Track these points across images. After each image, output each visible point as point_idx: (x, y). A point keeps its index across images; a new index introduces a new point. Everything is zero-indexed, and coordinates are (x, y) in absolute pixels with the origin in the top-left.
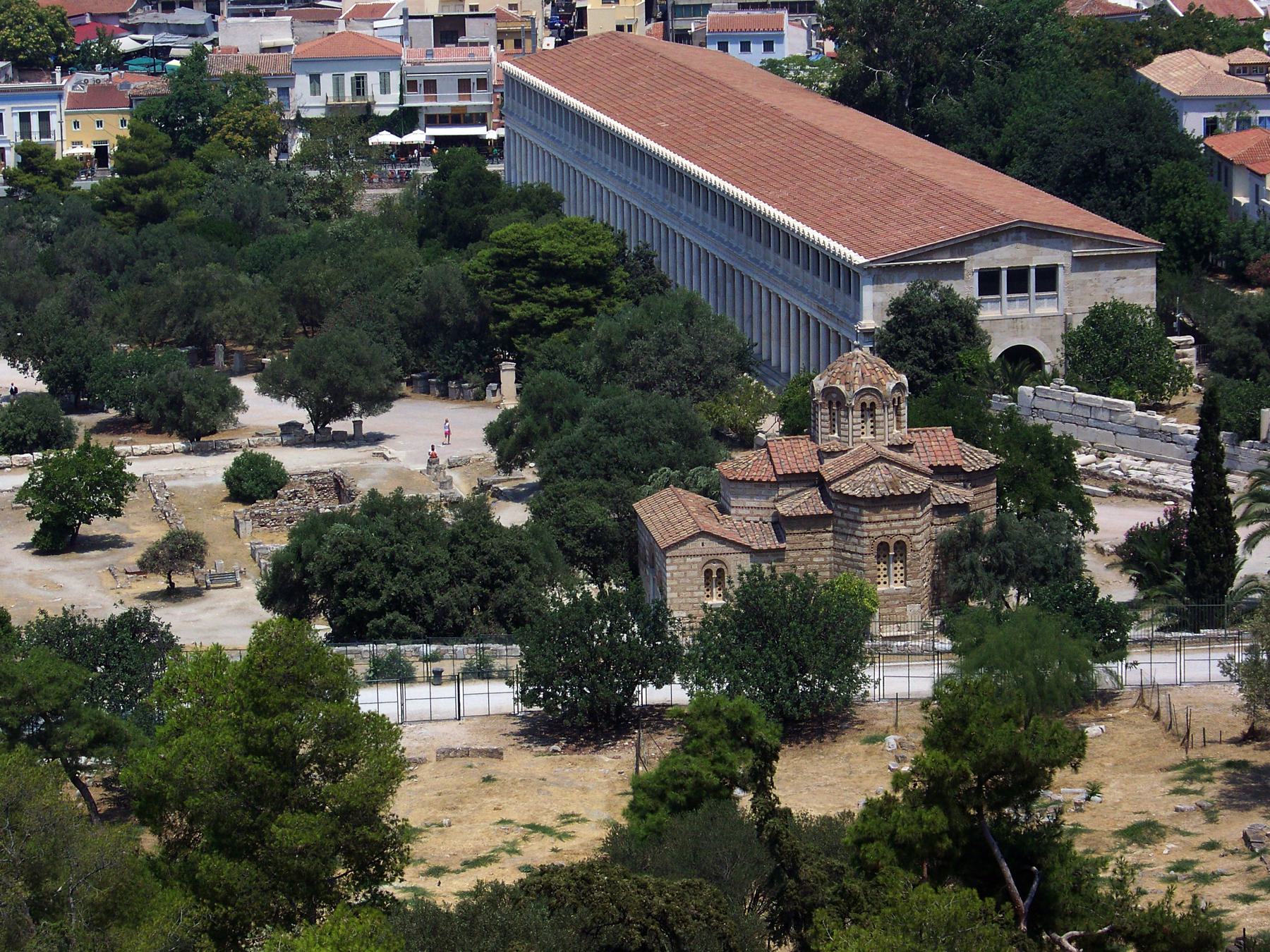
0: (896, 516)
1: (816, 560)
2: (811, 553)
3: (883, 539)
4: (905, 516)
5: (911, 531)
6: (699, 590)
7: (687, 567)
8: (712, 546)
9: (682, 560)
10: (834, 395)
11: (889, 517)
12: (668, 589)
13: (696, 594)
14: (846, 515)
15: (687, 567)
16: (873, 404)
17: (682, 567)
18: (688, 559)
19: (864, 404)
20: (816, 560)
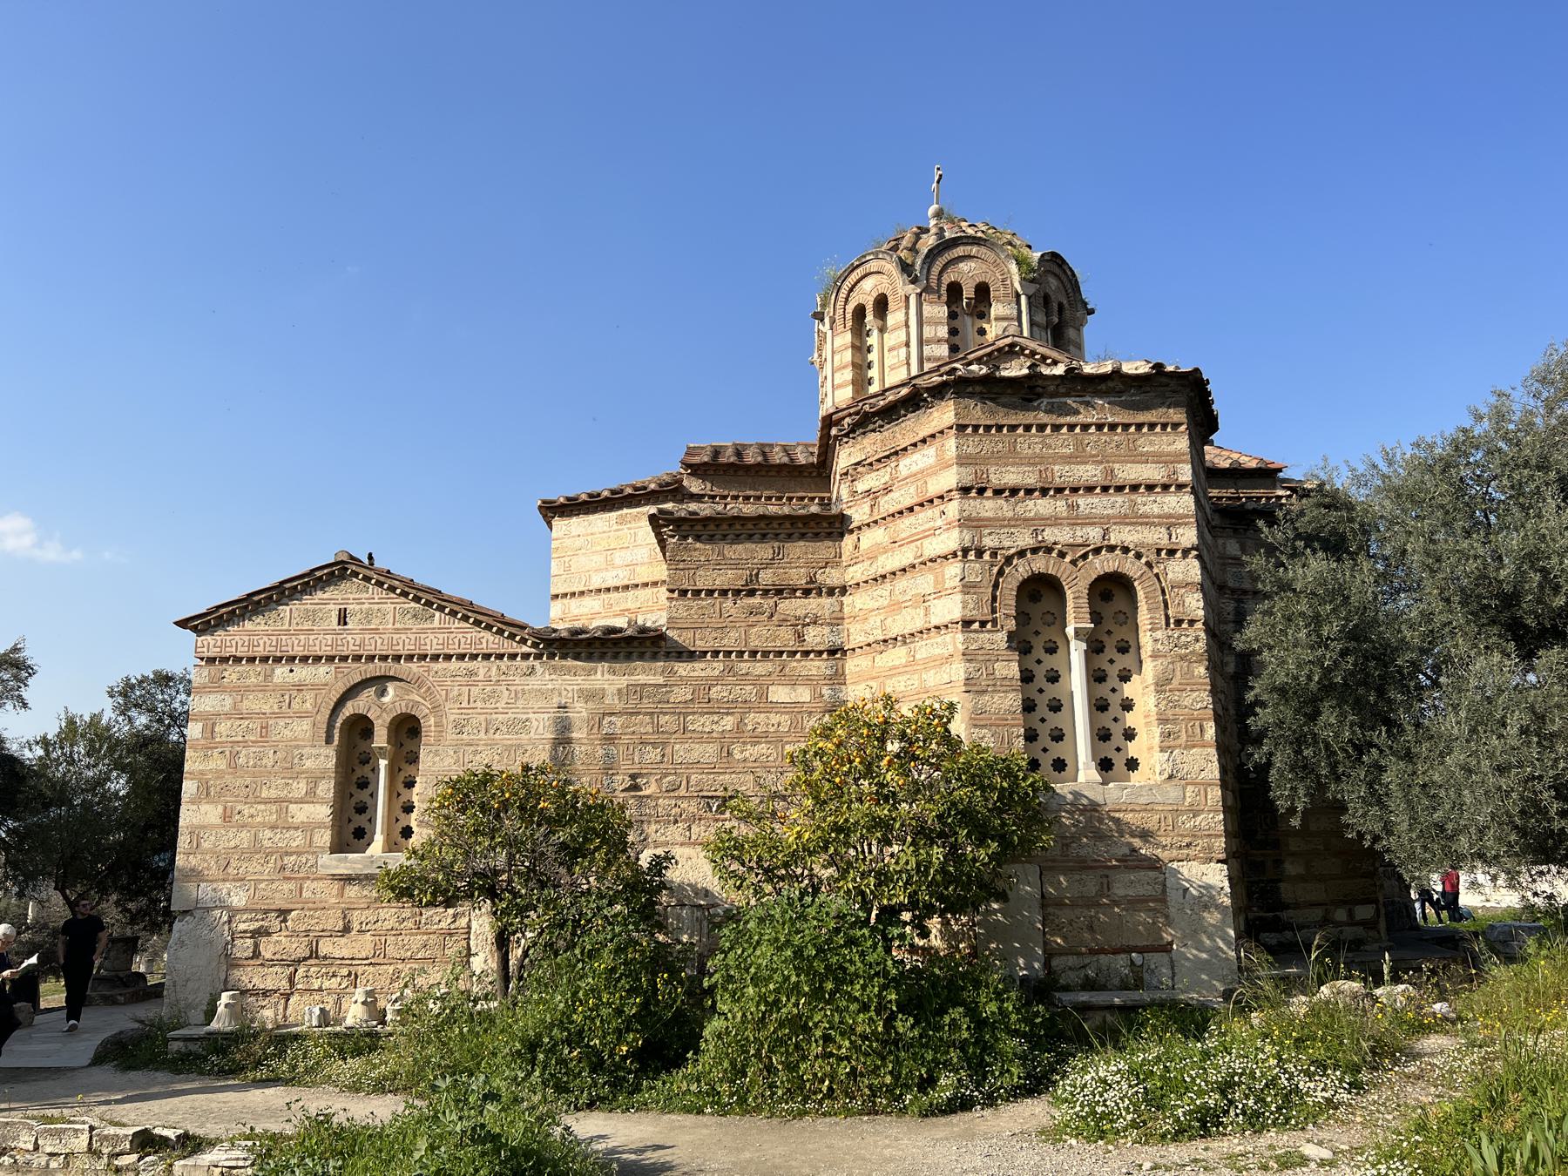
0: (1089, 473)
1: (779, 694)
2: (760, 668)
3: (1040, 564)
4: (1131, 473)
5: (1157, 536)
6: (310, 797)
7: (268, 705)
8: (380, 622)
9: (253, 674)
10: (868, 284)
11: (1064, 473)
12: (189, 787)
13: (300, 813)
14: (888, 504)
15: (268, 705)
16: (983, 291)
17: (252, 704)
18: (281, 672)
19: (955, 290)
20: (779, 694)
